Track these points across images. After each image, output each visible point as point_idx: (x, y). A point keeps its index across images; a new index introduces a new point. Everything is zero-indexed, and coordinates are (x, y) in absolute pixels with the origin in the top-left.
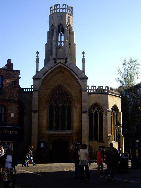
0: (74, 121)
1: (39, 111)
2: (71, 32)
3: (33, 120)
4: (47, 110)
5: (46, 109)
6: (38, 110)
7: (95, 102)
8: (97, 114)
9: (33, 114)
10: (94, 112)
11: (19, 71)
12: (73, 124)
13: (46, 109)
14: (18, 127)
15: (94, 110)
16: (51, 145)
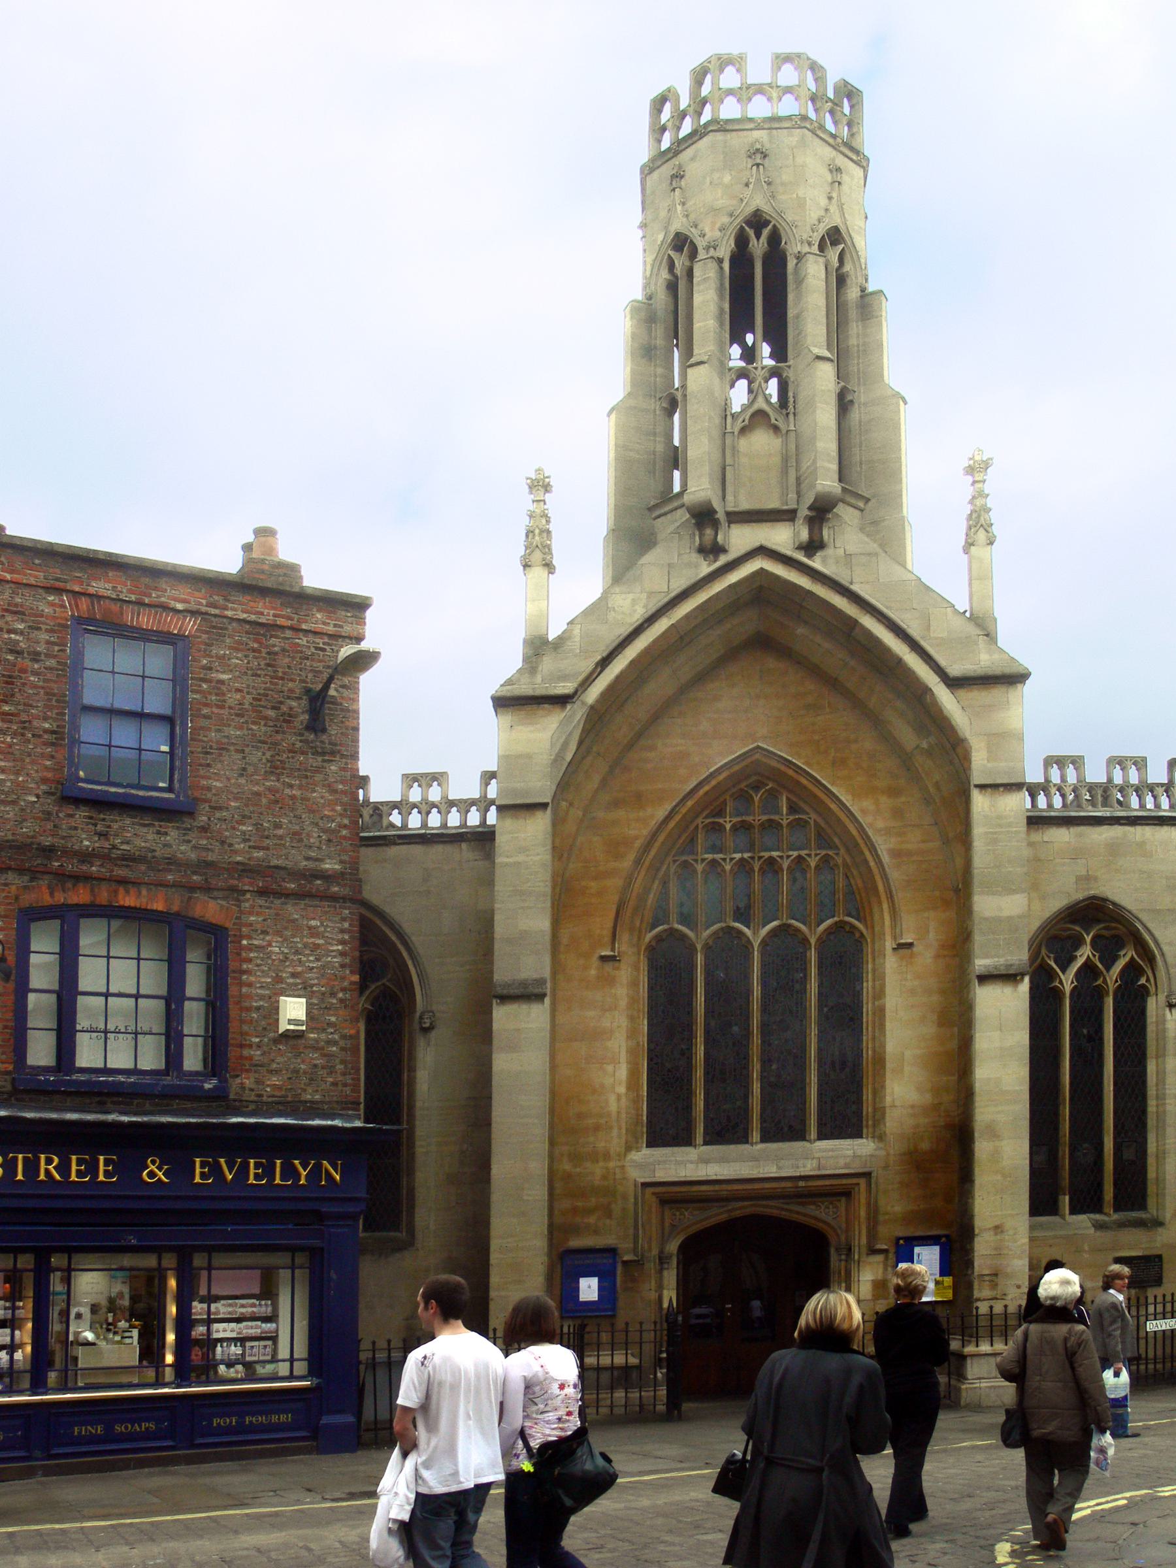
0: (889, 1065)
1: (554, 990)
2: (853, 294)
3: (502, 1063)
4: (634, 984)
5: (624, 973)
6: (547, 973)
7: (1080, 896)
8: (1100, 993)
9: (503, 1016)
10: (1067, 981)
11: (357, 606)
12: (879, 1090)
13: (624, 973)
14: (358, 1124)
15: (1072, 959)
16: (671, 1277)
